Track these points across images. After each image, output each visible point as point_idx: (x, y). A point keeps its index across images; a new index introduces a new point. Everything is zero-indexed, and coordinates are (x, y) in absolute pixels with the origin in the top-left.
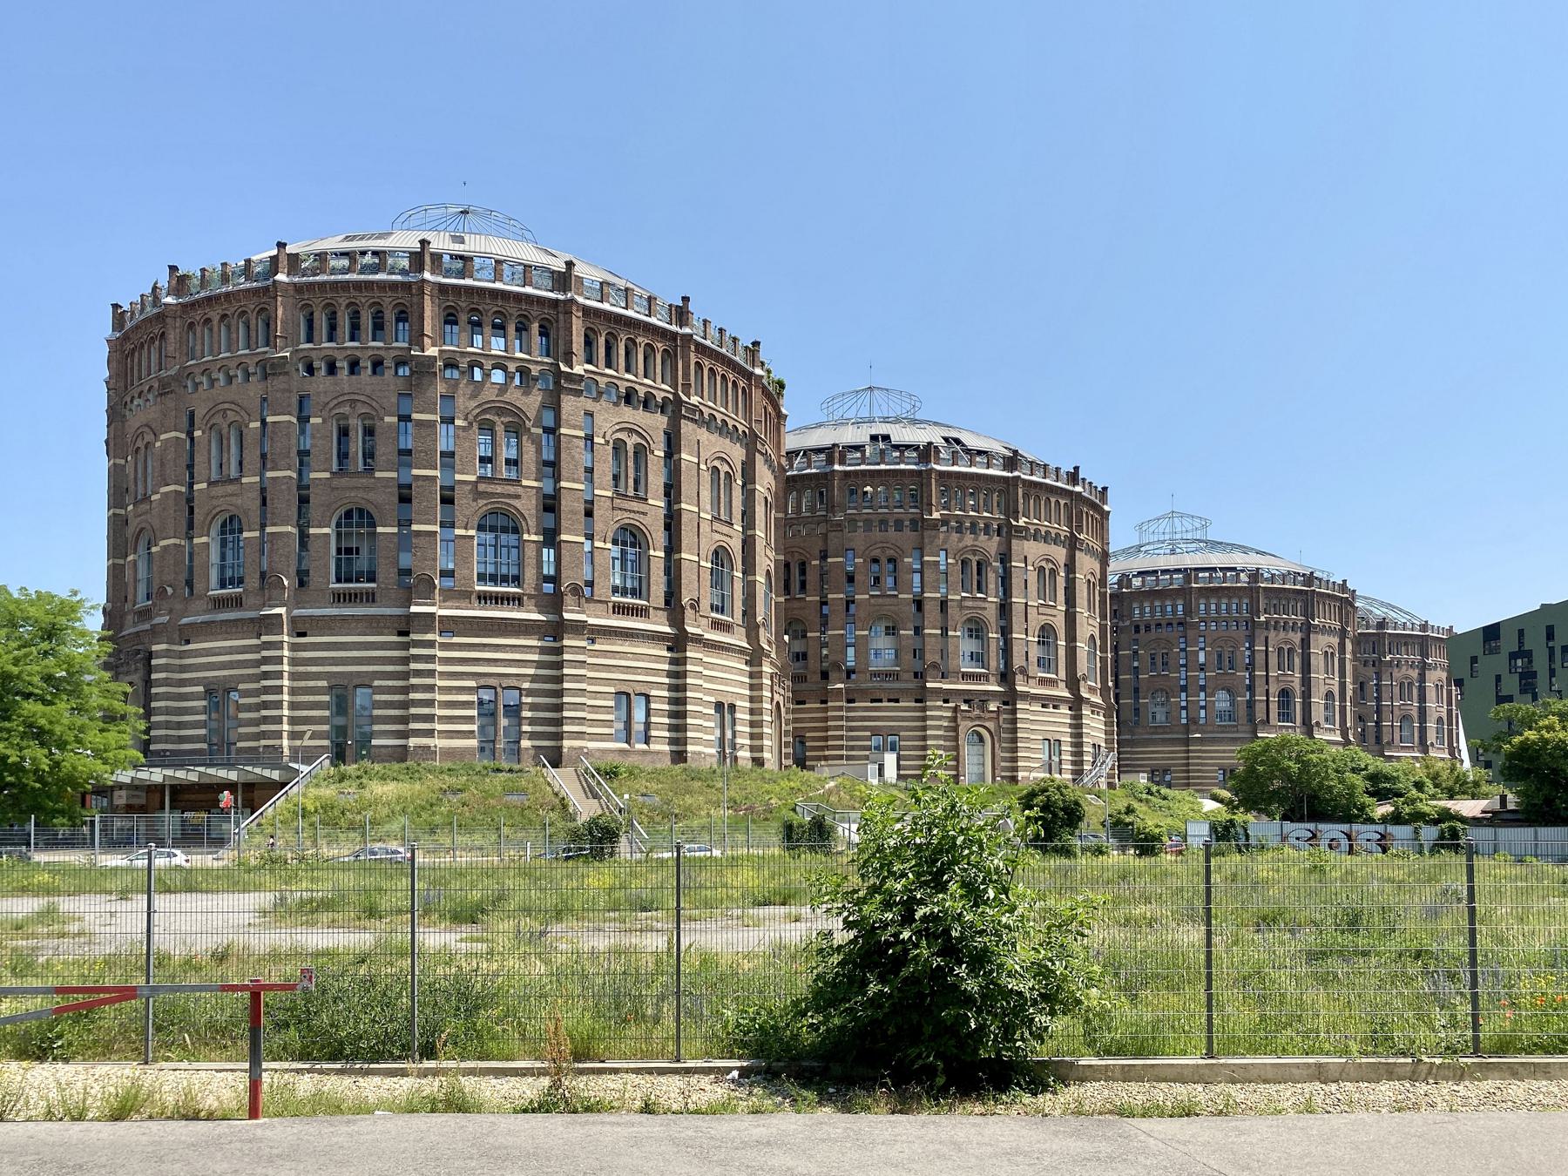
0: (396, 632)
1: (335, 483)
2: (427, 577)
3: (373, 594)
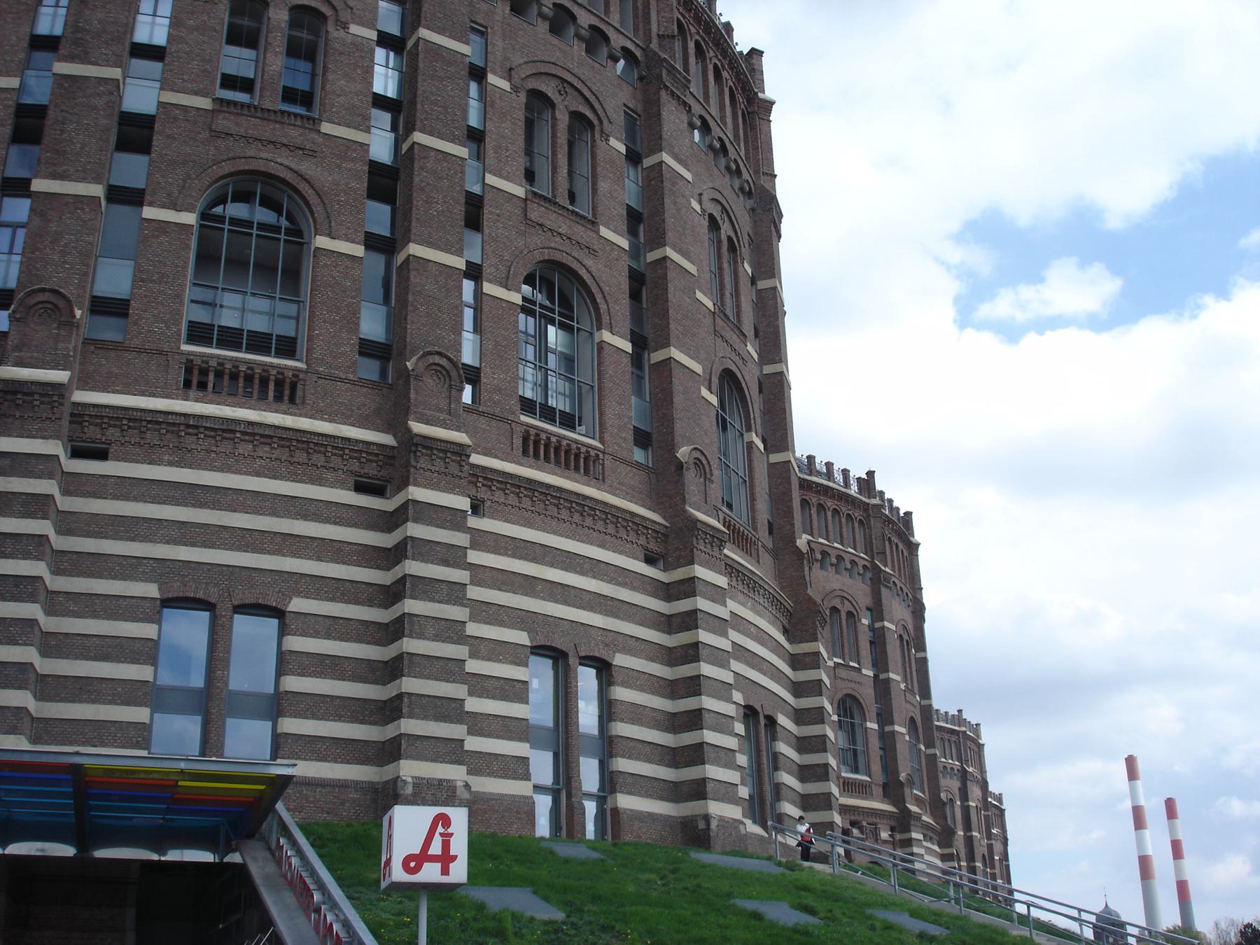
2: (444, 362)
3: (293, 387)
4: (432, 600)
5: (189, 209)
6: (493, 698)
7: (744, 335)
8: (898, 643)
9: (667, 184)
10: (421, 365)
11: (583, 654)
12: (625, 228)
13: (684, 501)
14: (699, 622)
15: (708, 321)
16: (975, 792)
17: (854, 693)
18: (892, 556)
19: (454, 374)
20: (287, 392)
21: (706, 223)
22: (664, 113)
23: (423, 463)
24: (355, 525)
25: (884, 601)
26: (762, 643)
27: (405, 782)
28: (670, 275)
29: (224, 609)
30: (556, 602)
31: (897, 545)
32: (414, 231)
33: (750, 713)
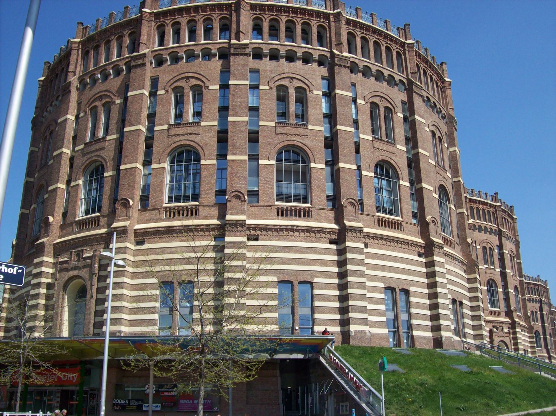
0: (328, 241)
1: (279, 130)
4: (355, 277)
5: (272, 159)
6: (375, 304)
7: (446, 171)
8: (509, 257)
9: (417, 126)
10: (346, 203)
11: (400, 288)
12: (405, 143)
13: (429, 235)
14: (436, 275)
15: (434, 169)
16: (546, 308)
17: (493, 278)
18: (506, 224)
19: (356, 204)
20: (307, 214)
21: (430, 134)
22: (415, 101)
23: (350, 234)
24: (331, 254)
25: (503, 242)
26: (457, 277)
27: (352, 332)
28: (421, 158)
29: (296, 283)
30: (391, 272)
31: (508, 220)
32: (340, 159)
33: (454, 301)
